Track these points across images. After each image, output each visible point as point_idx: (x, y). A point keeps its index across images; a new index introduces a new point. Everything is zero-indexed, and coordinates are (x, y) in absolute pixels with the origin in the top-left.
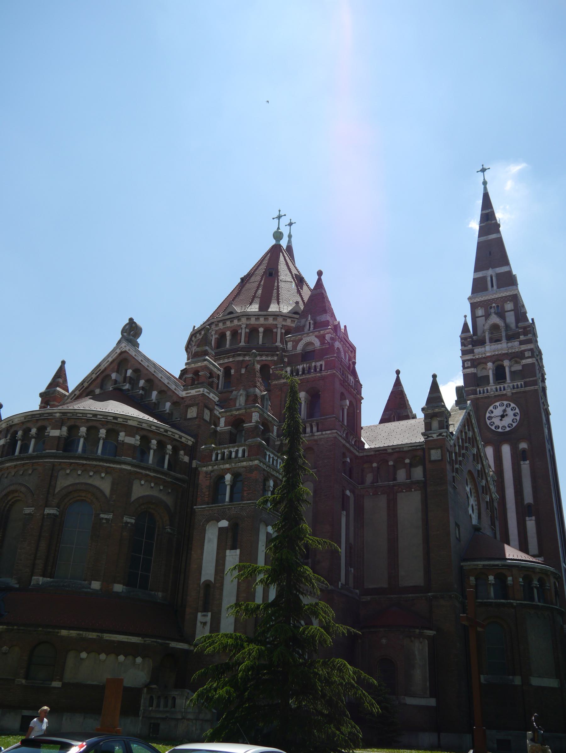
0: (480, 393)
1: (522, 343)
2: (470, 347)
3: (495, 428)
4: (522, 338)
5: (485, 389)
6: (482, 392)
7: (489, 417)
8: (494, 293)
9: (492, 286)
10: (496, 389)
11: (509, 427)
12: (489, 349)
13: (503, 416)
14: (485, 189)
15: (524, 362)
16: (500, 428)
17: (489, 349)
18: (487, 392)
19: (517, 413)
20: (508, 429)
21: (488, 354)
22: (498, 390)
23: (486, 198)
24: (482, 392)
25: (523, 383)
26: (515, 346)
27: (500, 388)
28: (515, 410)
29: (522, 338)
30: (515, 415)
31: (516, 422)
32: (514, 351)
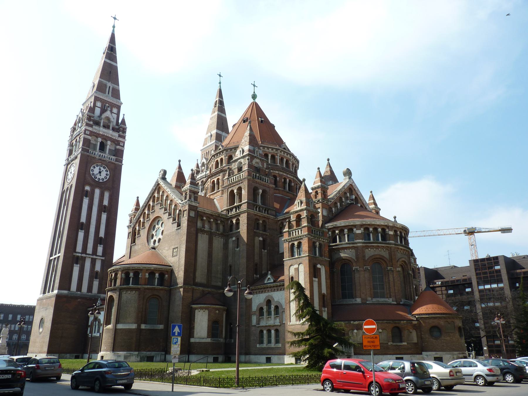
0: (90, 153)
1: (120, 136)
2: (91, 123)
3: (95, 178)
4: (121, 133)
5: (94, 152)
6: (91, 153)
7: (92, 170)
8: (108, 97)
9: (108, 93)
10: (100, 155)
11: (102, 180)
12: (102, 130)
13: (100, 172)
14: (113, 30)
15: (118, 147)
16: (97, 178)
17: (102, 130)
18: (95, 154)
19: (108, 174)
20: (101, 181)
21: (101, 133)
22: (101, 156)
24: (91, 153)
25: (115, 159)
26: (115, 135)
27: (102, 155)
28: (107, 172)
29: (121, 133)
30: (106, 174)
31: (106, 179)
32: (115, 138)
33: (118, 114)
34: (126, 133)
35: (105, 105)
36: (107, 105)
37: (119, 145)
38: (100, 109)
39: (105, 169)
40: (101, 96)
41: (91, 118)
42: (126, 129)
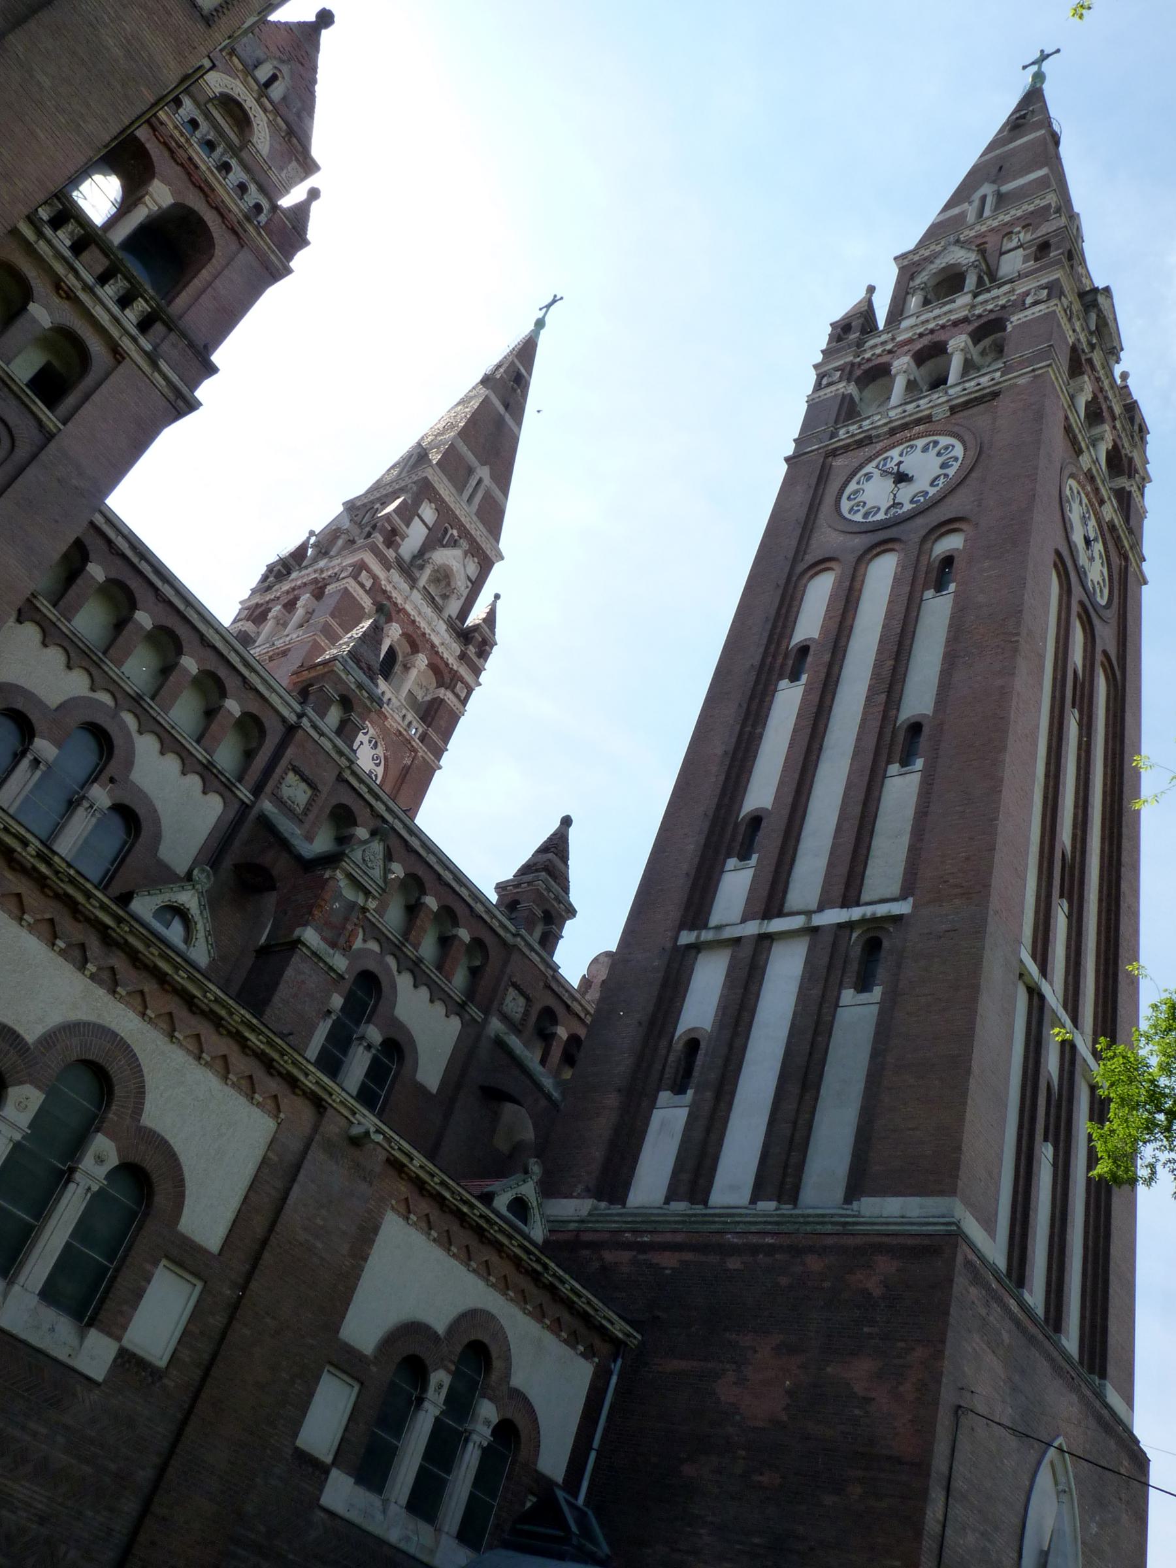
8: (466, 513)
9: (470, 500)
17: (414, 603)
19: (376, 776)
23: (526, 351)
26: (450, 650)
28: (378, 765)
33: (476, 585)
34: (486, 661)
35: (446, 531)
36: (455, 532)
37: (451, 687)
38: (427, 531)
39: (374, 752)
40: (445, 489)
41: (398, 538)
42: (492, 649)
